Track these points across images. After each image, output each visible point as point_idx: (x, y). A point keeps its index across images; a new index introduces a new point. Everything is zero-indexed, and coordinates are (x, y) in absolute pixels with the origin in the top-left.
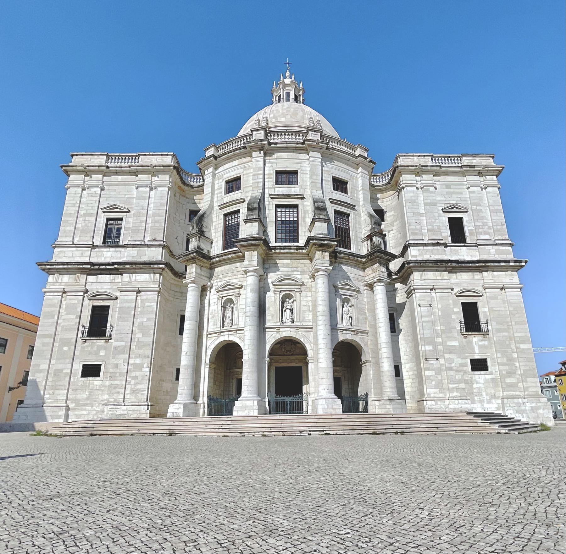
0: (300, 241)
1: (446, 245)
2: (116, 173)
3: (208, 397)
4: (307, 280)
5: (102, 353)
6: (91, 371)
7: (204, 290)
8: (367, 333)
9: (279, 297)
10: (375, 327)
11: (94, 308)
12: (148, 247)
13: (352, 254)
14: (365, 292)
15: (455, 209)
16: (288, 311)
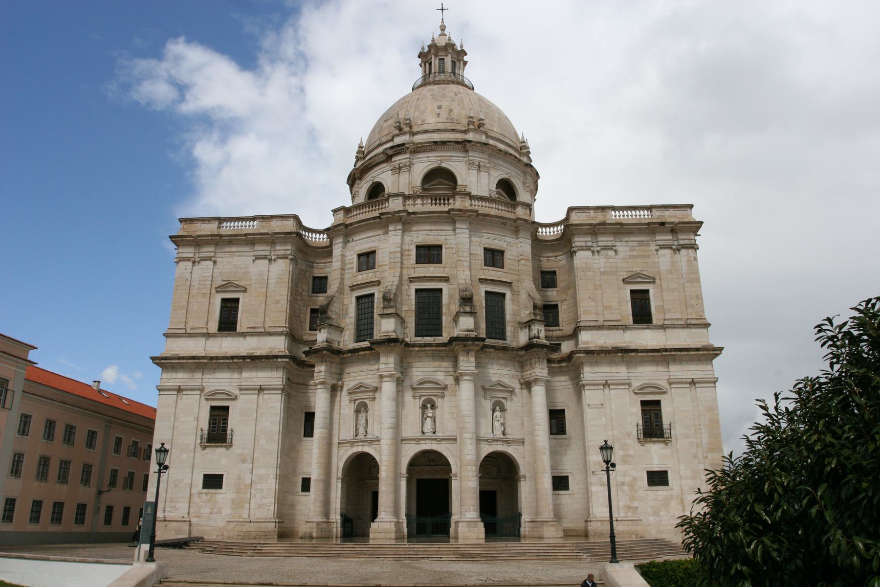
0: (444, 334)
1: (625, 328)
3: (341, 515)
4: (450, 381)
6: (213, 481)
7: (334, 390)
8: (522, 442)
9: (419, 403)
10: (532, 433)
11: (213, 408)
12: (270, 334)
13: (505, 349)
14: (521, 394)
15: (639, 280)
16: (429, 420)
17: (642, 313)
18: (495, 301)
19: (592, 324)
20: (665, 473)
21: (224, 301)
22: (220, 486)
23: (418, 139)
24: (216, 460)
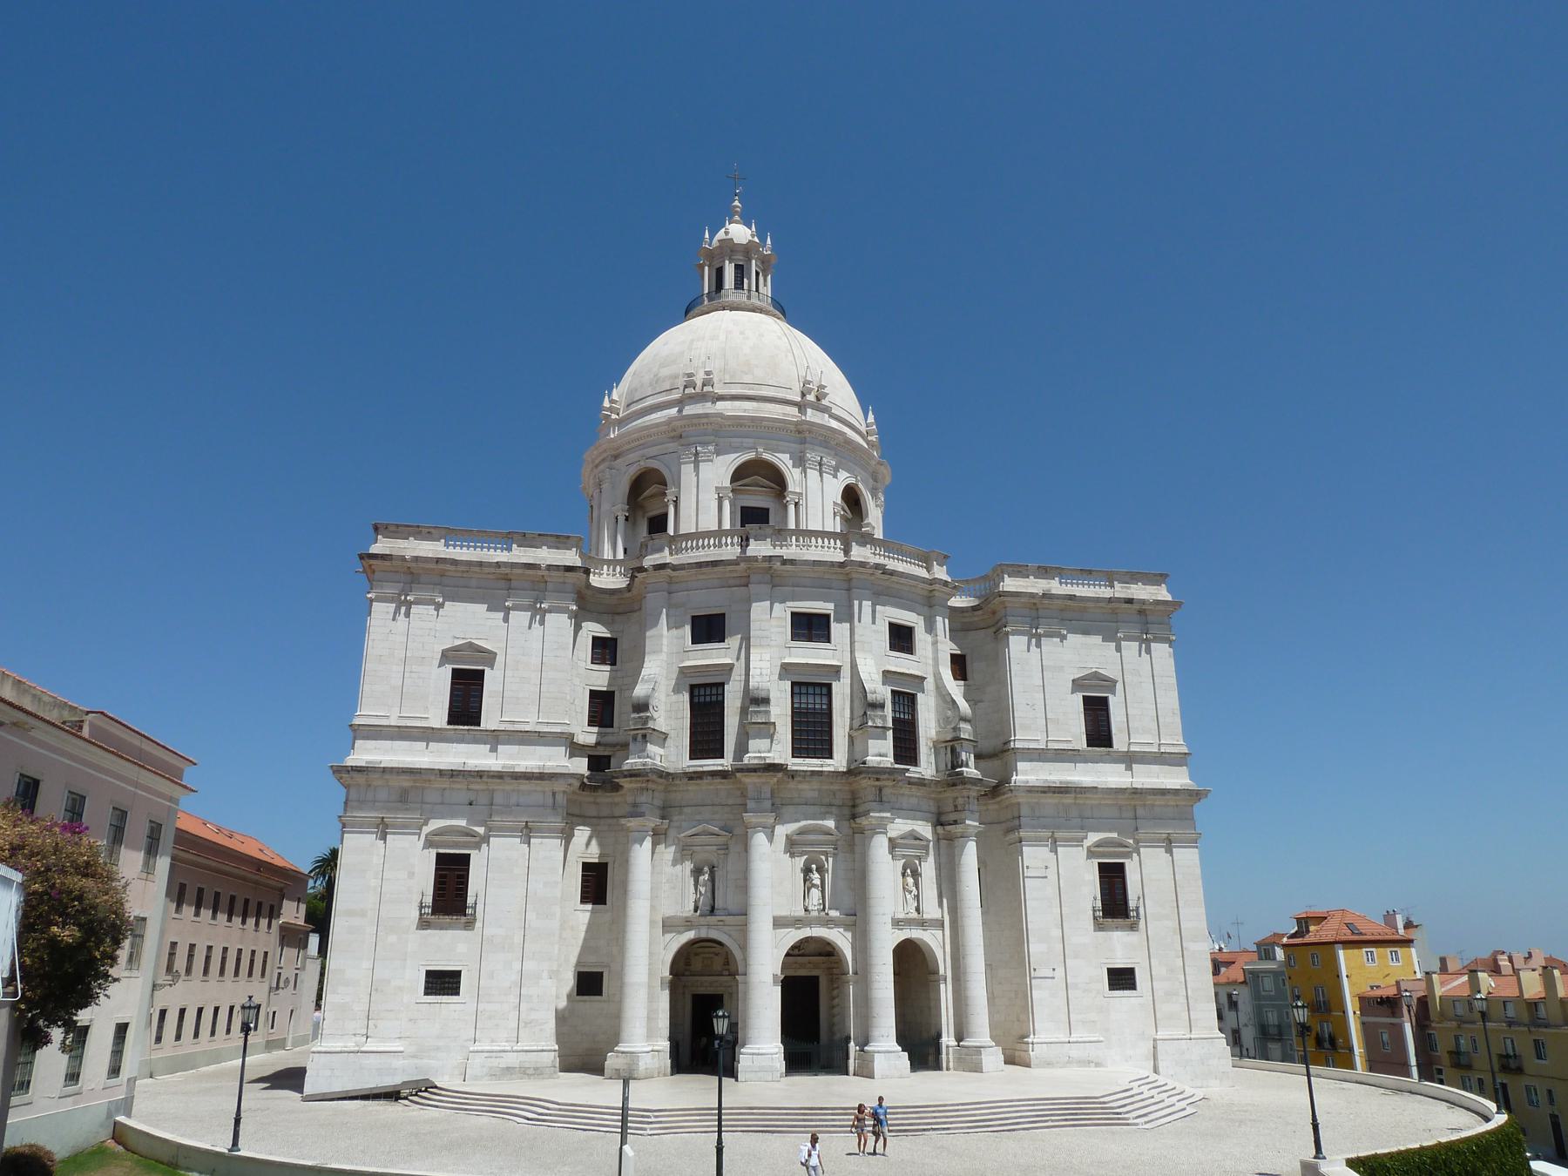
5: (462, 948)
6: (443, 983)
9: (800, 862)
15: (1094, 682)
17: (1099, 732)
18: (905, 701)
20: (1131, 971)
21: (457, 674)
22: (458, 994)
24: (449, 947)
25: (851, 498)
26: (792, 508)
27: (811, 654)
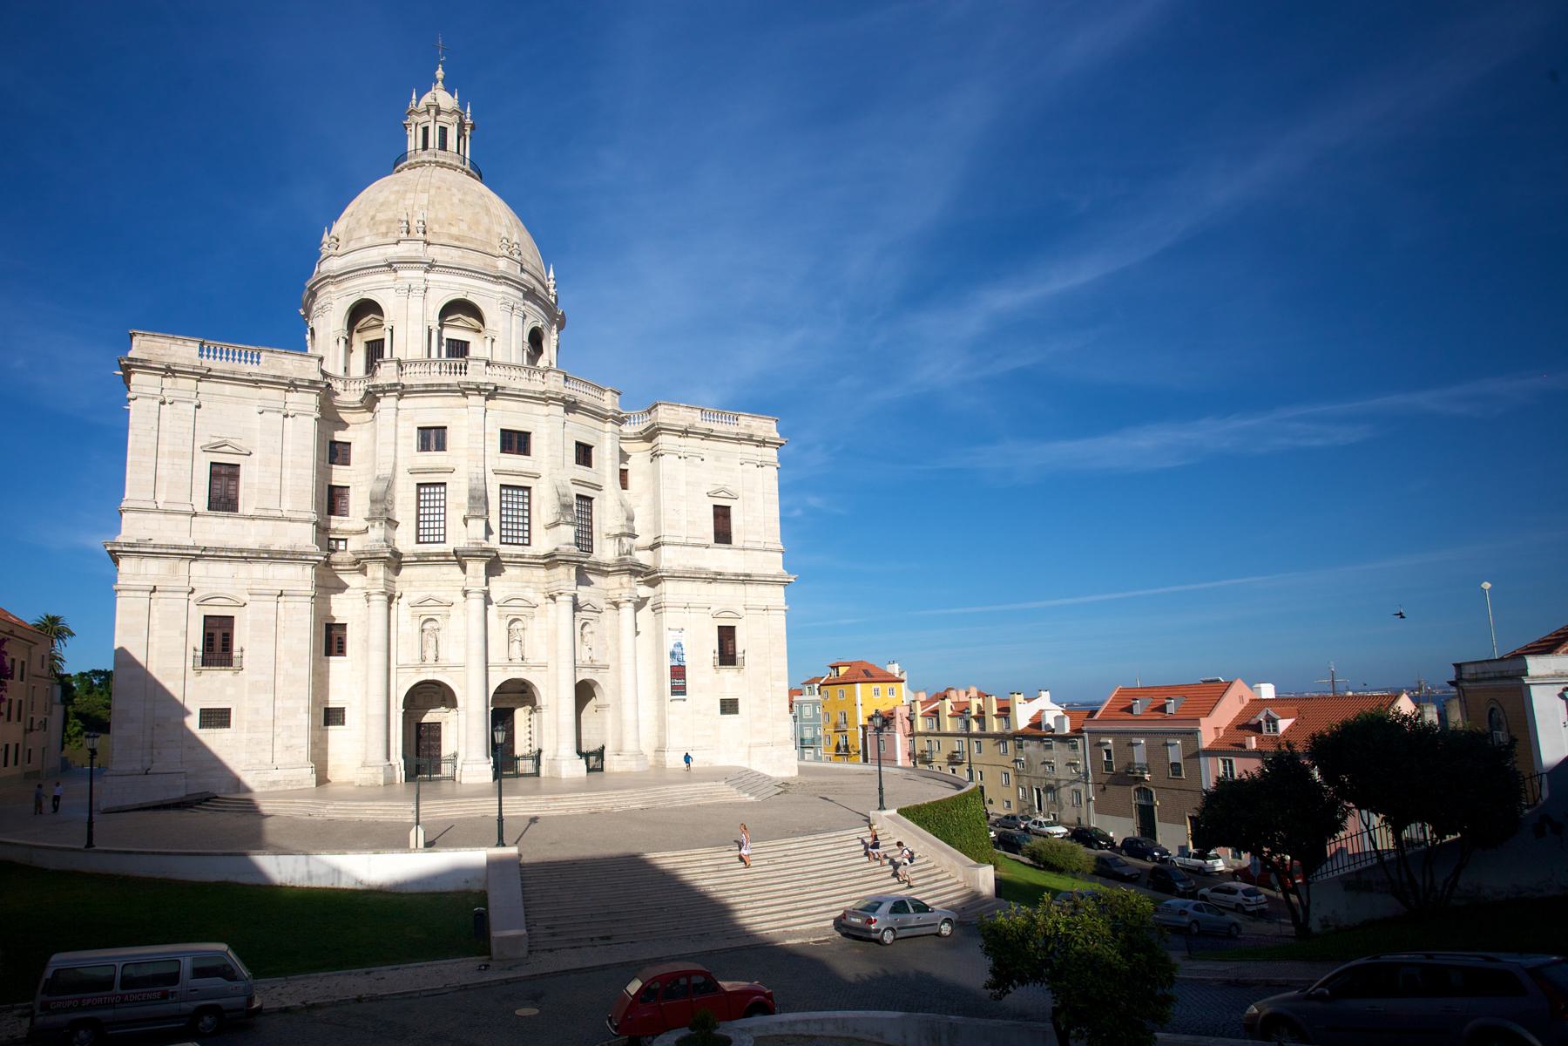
2: (222, 378)
4: (540, 599)
5: (230, 691)
10: (619, 659)
19: (677, 540)
23: (434, 253)
25: (536, 339)
26: (488, 341)
27: (514, 461)
